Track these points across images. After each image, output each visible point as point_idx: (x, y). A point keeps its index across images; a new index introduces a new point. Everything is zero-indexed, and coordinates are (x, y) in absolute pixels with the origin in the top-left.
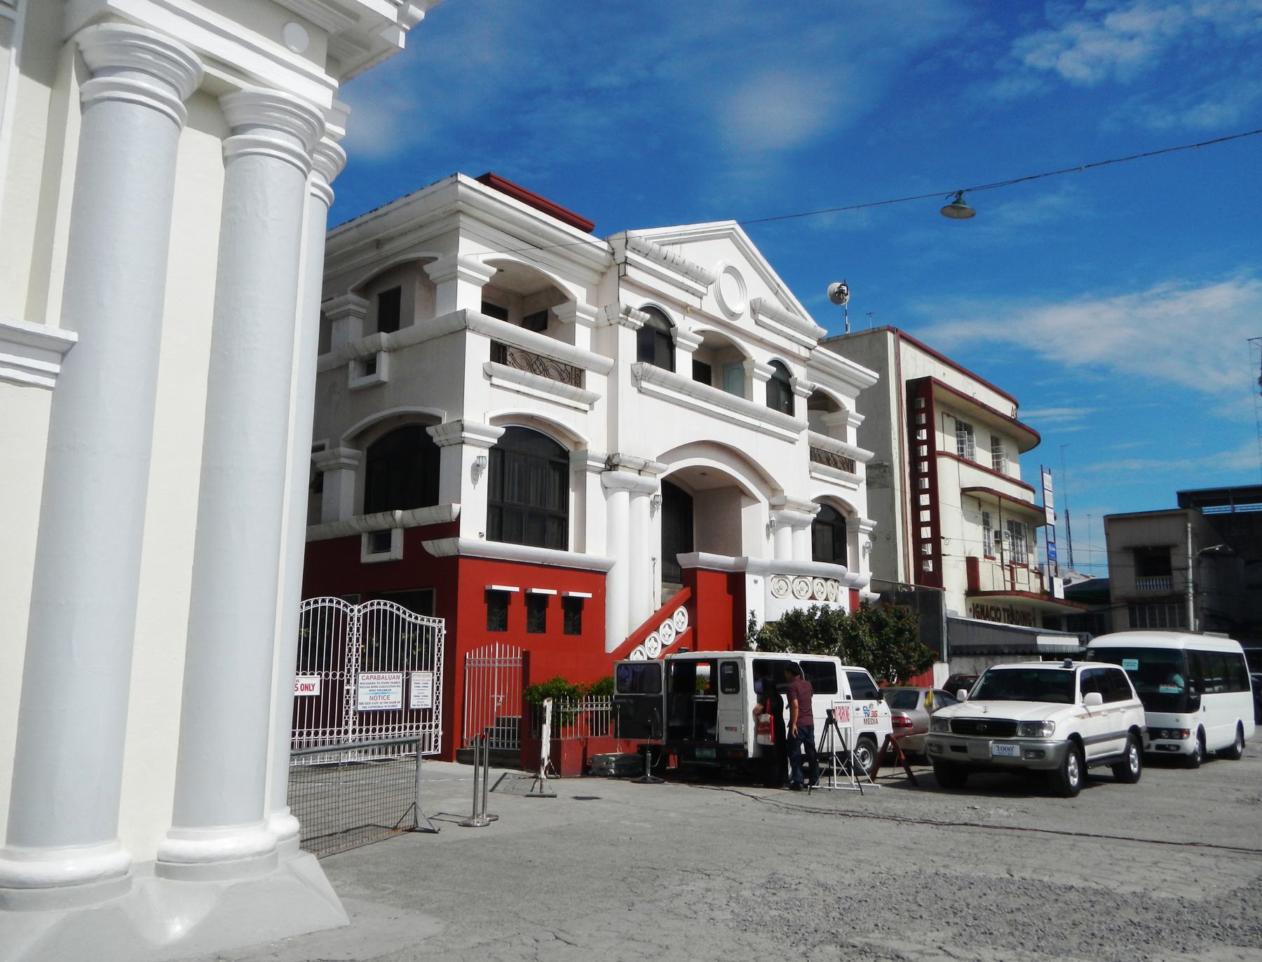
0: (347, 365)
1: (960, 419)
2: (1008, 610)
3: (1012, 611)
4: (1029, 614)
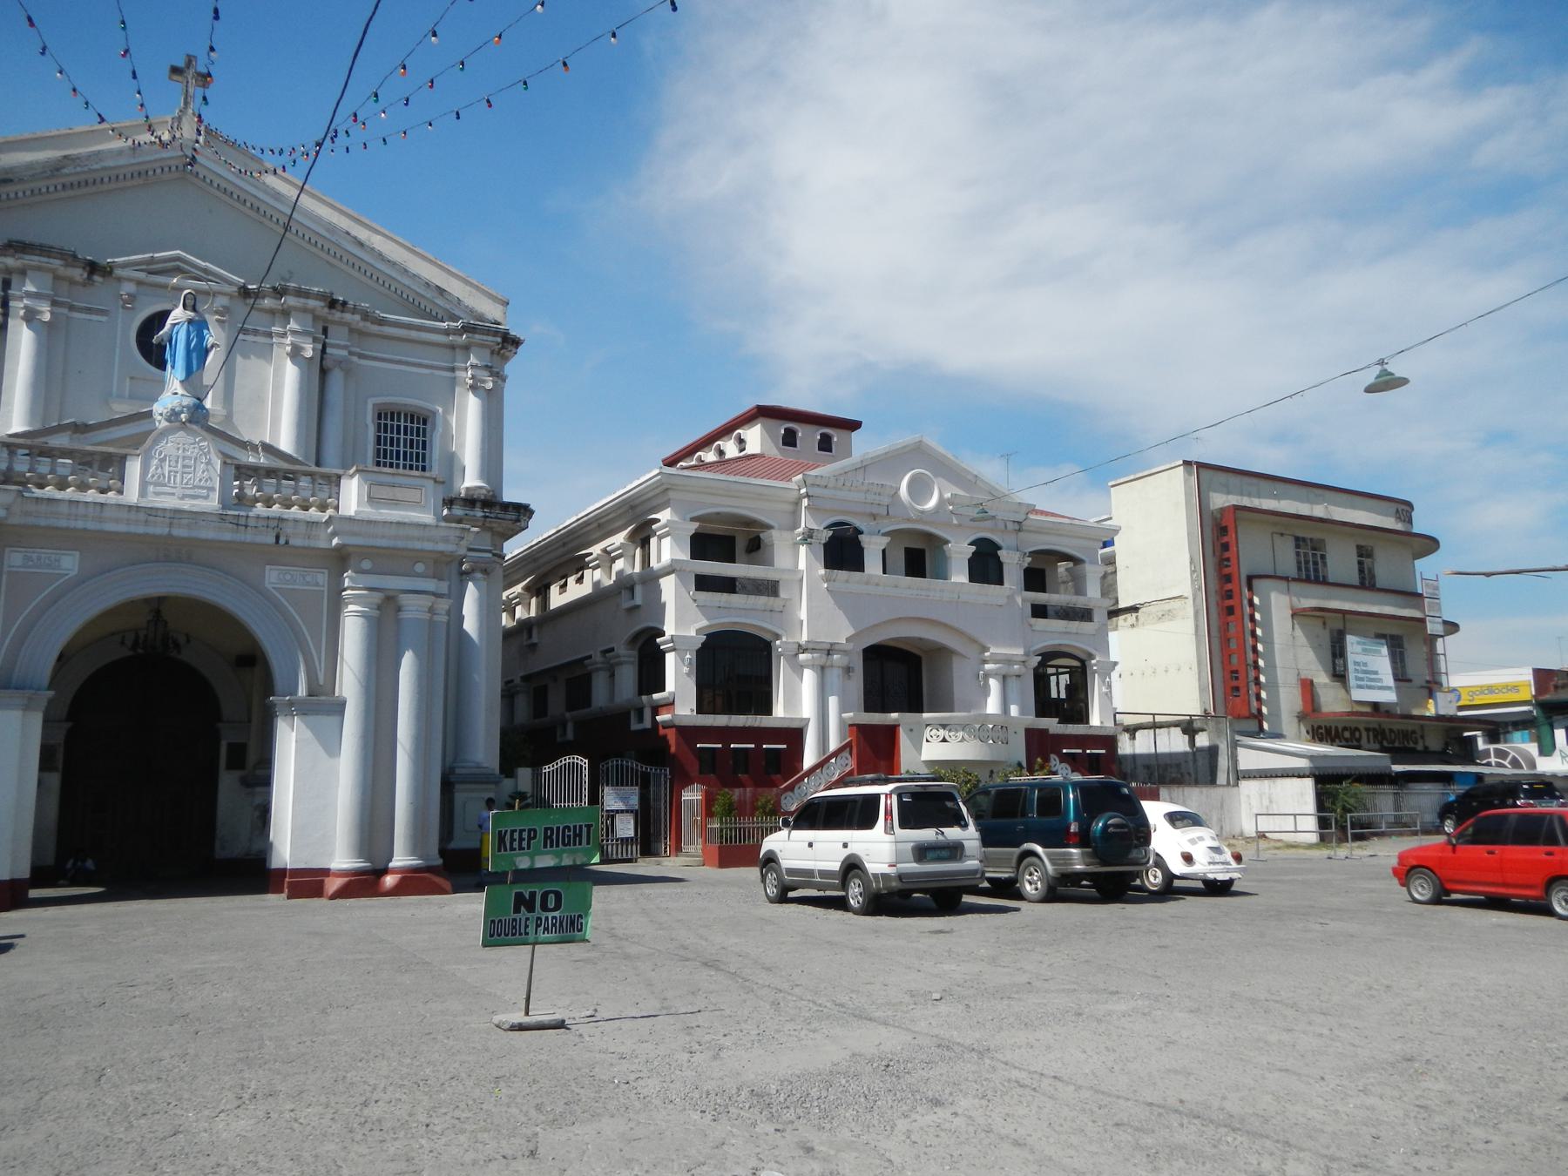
0: (620, 593)
1: (1300, 534)
2: (1374, 730)
3: (1384, 730)
4: (1414, 732)
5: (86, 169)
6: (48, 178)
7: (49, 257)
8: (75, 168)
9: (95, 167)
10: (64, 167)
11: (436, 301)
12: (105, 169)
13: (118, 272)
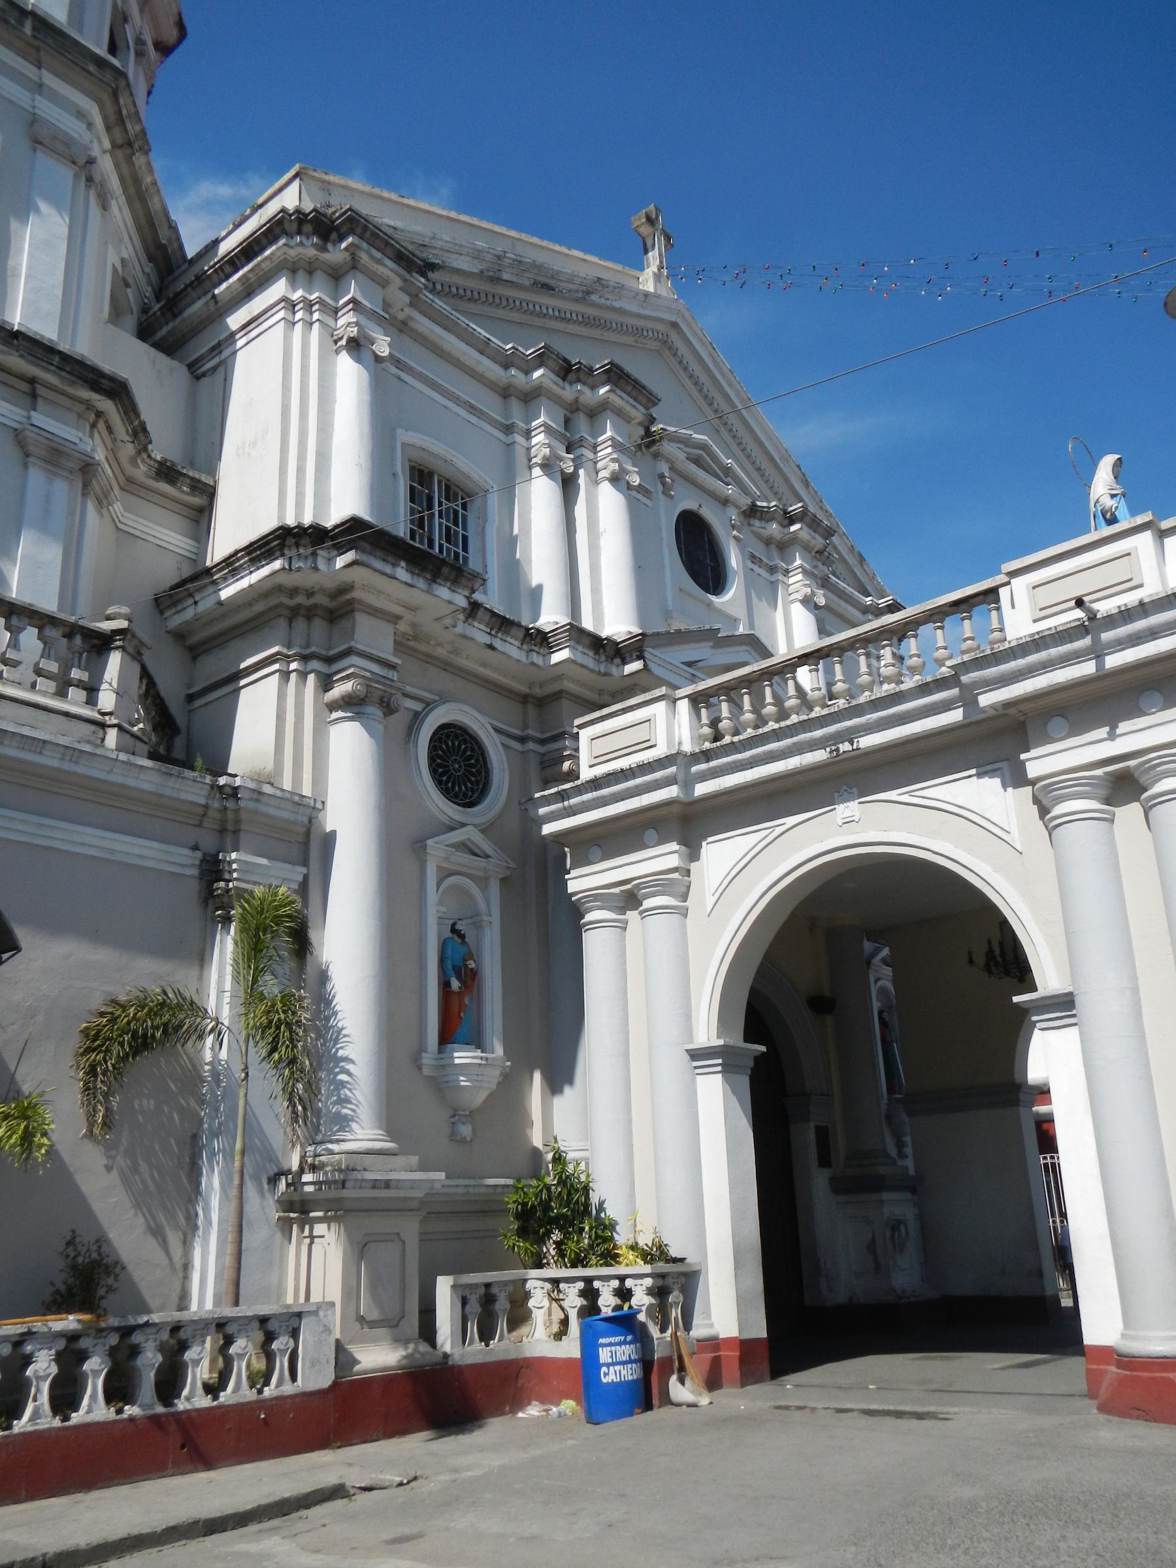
5: (608, 303)
6: (577, 300)
7: (635, 399)
8: (600, 297)
9: (617, 304)
10: (592, 293)
11: (856, 570)
12: (621, 311)
13: (667, 448)
